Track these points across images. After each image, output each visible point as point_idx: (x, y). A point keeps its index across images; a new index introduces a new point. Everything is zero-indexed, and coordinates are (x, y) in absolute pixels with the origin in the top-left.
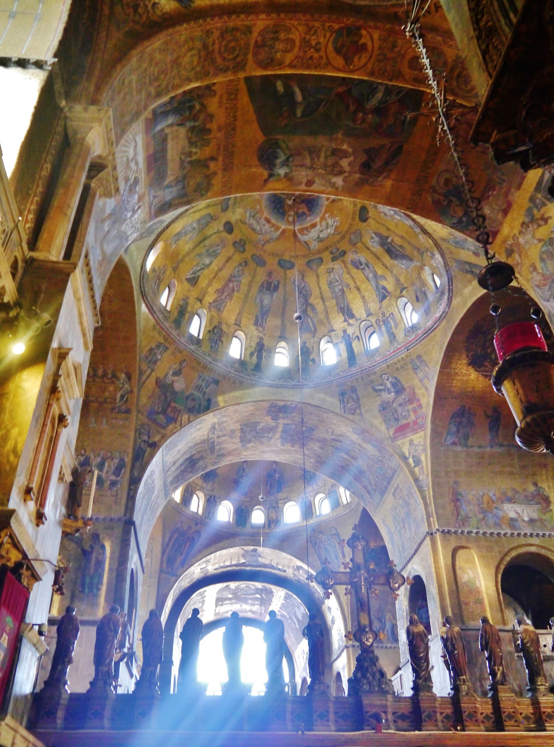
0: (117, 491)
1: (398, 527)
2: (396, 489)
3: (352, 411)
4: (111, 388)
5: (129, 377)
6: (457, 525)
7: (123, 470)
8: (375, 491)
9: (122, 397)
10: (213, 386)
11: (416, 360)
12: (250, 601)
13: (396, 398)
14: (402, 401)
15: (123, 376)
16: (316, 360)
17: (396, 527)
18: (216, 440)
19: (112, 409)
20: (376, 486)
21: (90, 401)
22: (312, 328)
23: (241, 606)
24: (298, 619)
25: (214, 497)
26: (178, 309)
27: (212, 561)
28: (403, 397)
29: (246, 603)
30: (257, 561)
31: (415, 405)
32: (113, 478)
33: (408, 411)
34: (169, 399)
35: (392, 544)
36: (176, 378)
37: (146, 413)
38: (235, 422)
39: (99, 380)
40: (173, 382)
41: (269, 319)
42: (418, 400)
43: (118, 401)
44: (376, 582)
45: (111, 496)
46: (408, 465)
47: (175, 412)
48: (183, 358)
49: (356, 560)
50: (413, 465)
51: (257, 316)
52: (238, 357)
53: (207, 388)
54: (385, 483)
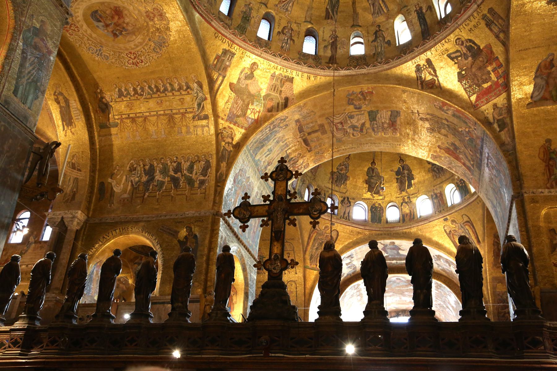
0: (205, 189)
1: (498, 199)
2: (488, 159)
3: (430, 86)
4: (188, 98)
5: (200, 86)
6: (548, 185)
7: (209, 170)
8: (473, 165)
9: (199, 105)
10: (287, 84)
11: (488, 15)
12: (406, 293)
13: (473, 63)
14: (481, 64)
15: (196, 85)
16: (391, 41)
17: (497, 200)
18: (308, 137)
19: (194, 118)
20: (473, 161)
21: (174, 114)
22: (385, 10)
23: (400, 299)
24: (453, 307)
25: (348, 198)
26: (241, 16)
27: (354, 256)
28: (481, 59)
29: (404, 296)
30: (398, 253)
31: (494, 65)
32: (202, 178)
33: (489, 73)
34: (246, 103)
35: (497, 218)
36: (249, 82)
37: (226, 118)
38: (320, 117)
39: (178, 93)
40: (247, 85)
41: (340, 9)
42: (497, 58)
43: (197, 110)
44: (295, 211)
45: (201, 193)
46: (492, 131)
47: (254, 114)
48: (253, 61)
49: (276, 192)
50: (498, 129)
51: (327, 8)
52: (314, 54)
53: (282, 87)
54: (478, 155)
